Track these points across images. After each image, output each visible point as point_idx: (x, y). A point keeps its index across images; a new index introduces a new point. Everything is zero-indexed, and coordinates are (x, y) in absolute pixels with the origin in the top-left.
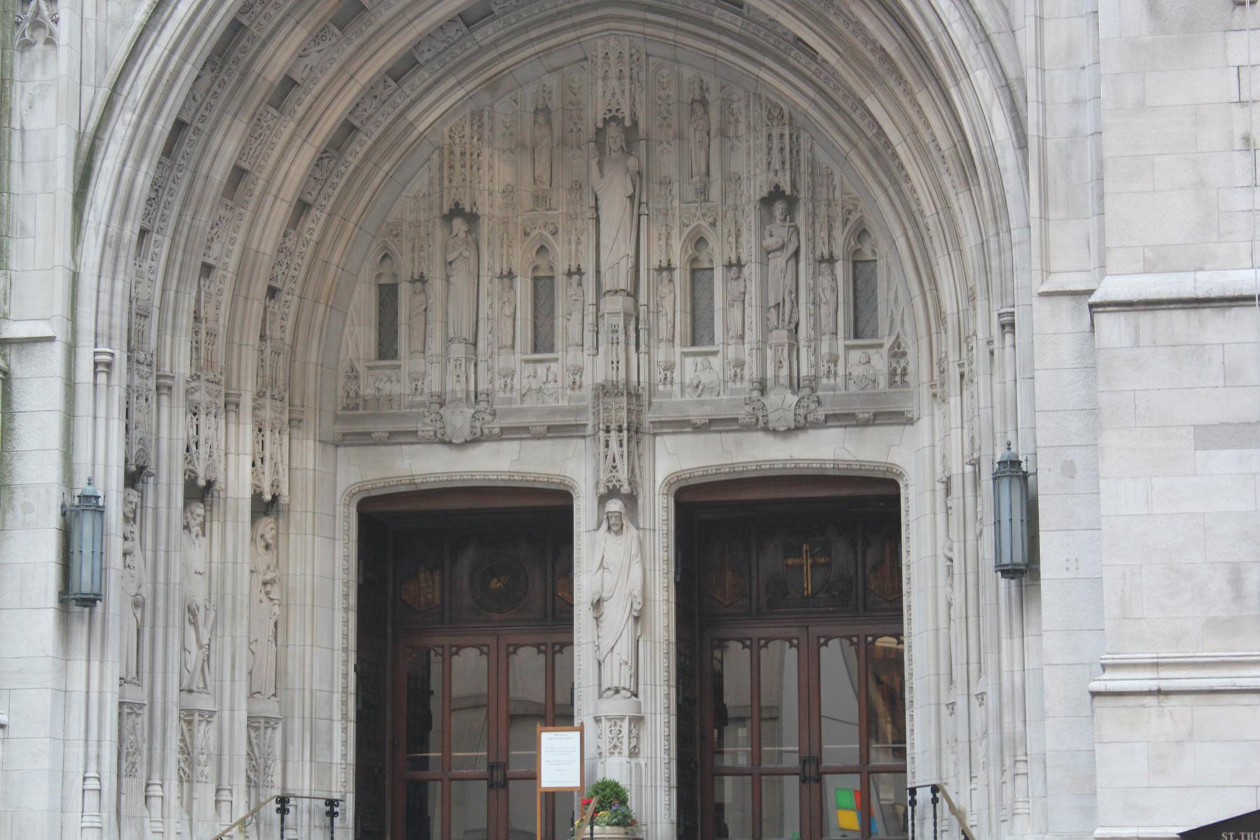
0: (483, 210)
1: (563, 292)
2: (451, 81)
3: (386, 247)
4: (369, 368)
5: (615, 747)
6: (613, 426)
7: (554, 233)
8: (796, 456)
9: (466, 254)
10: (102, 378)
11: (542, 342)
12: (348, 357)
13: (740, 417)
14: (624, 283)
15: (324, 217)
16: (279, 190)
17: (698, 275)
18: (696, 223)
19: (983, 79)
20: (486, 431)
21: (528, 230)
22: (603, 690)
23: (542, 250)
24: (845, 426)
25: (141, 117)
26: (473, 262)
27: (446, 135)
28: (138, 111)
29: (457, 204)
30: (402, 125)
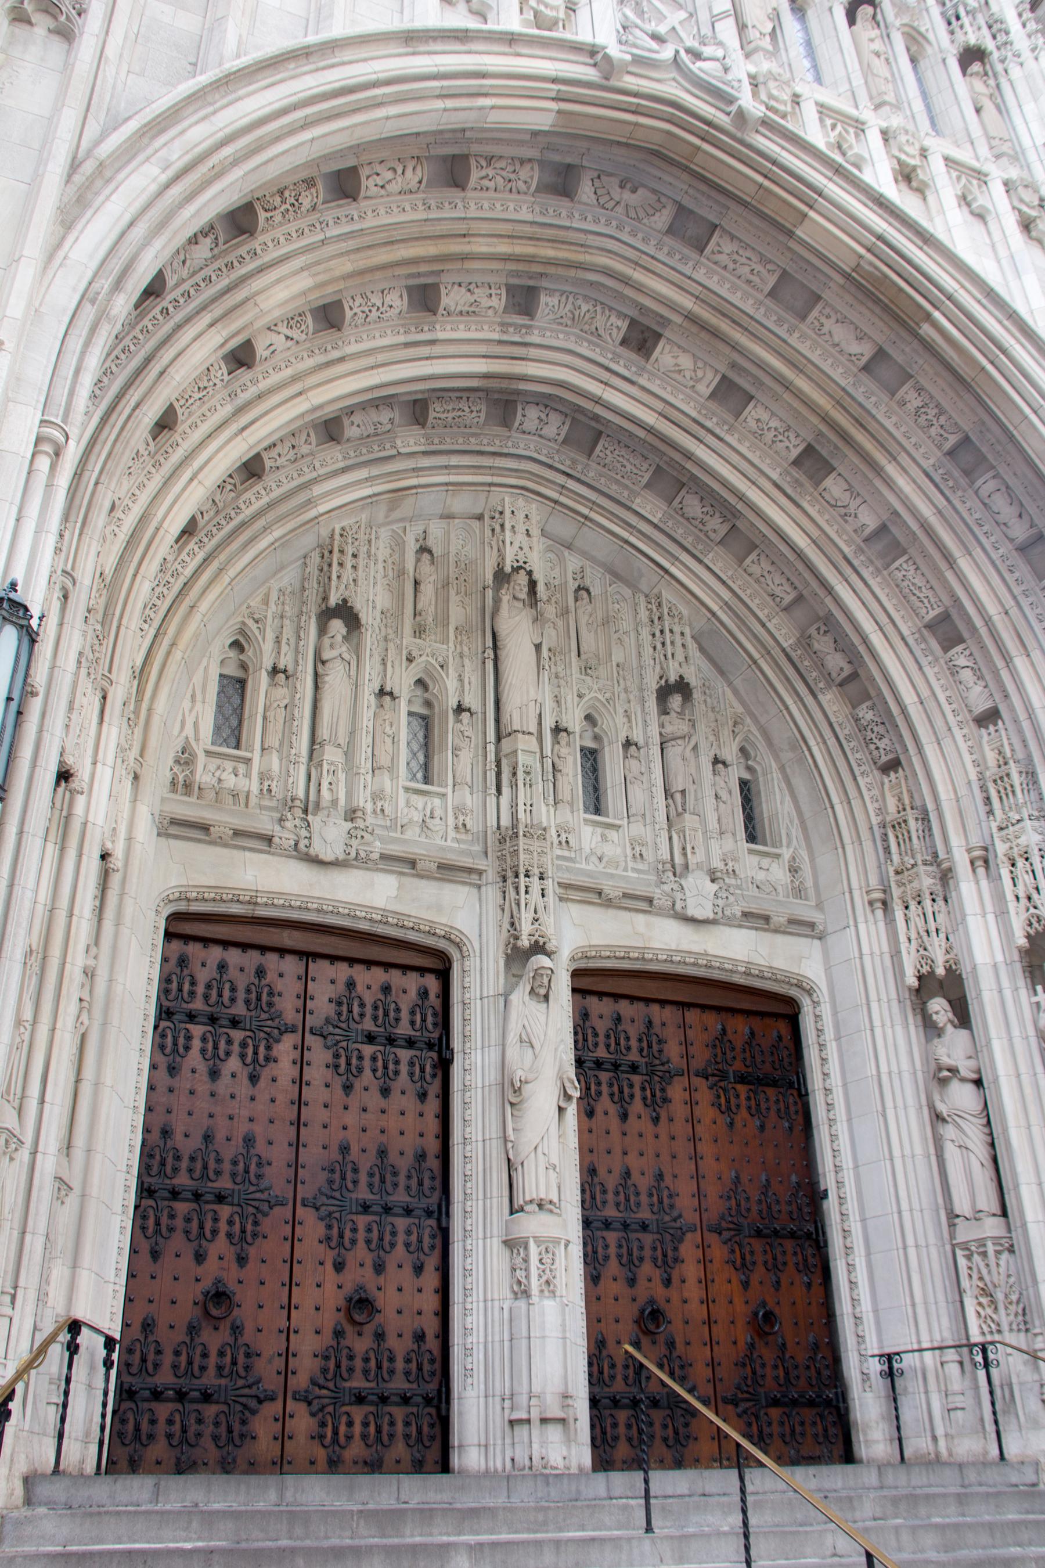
0: (368, 617)
1: (451, 730)
2: (362, 473)
3: (242, 632)
4: (208, 753)
5: (548, 1282)
6: (536, 871)
8: (711, 952)
9: (346, 656)
10: (44, 463)
12: (184, 734)
13: (656, 896)
15: (201, 556)
16: (201, 468)
18: (593, 694)
20: (363, 854)
21: (414, 654)
22: (519, 1201)
24: (757, 929)
25: (167, 186)
26: (354, 664)
27: (337, 532)
28: (170, 173)
29: (345, 601)
30: (302, 497)
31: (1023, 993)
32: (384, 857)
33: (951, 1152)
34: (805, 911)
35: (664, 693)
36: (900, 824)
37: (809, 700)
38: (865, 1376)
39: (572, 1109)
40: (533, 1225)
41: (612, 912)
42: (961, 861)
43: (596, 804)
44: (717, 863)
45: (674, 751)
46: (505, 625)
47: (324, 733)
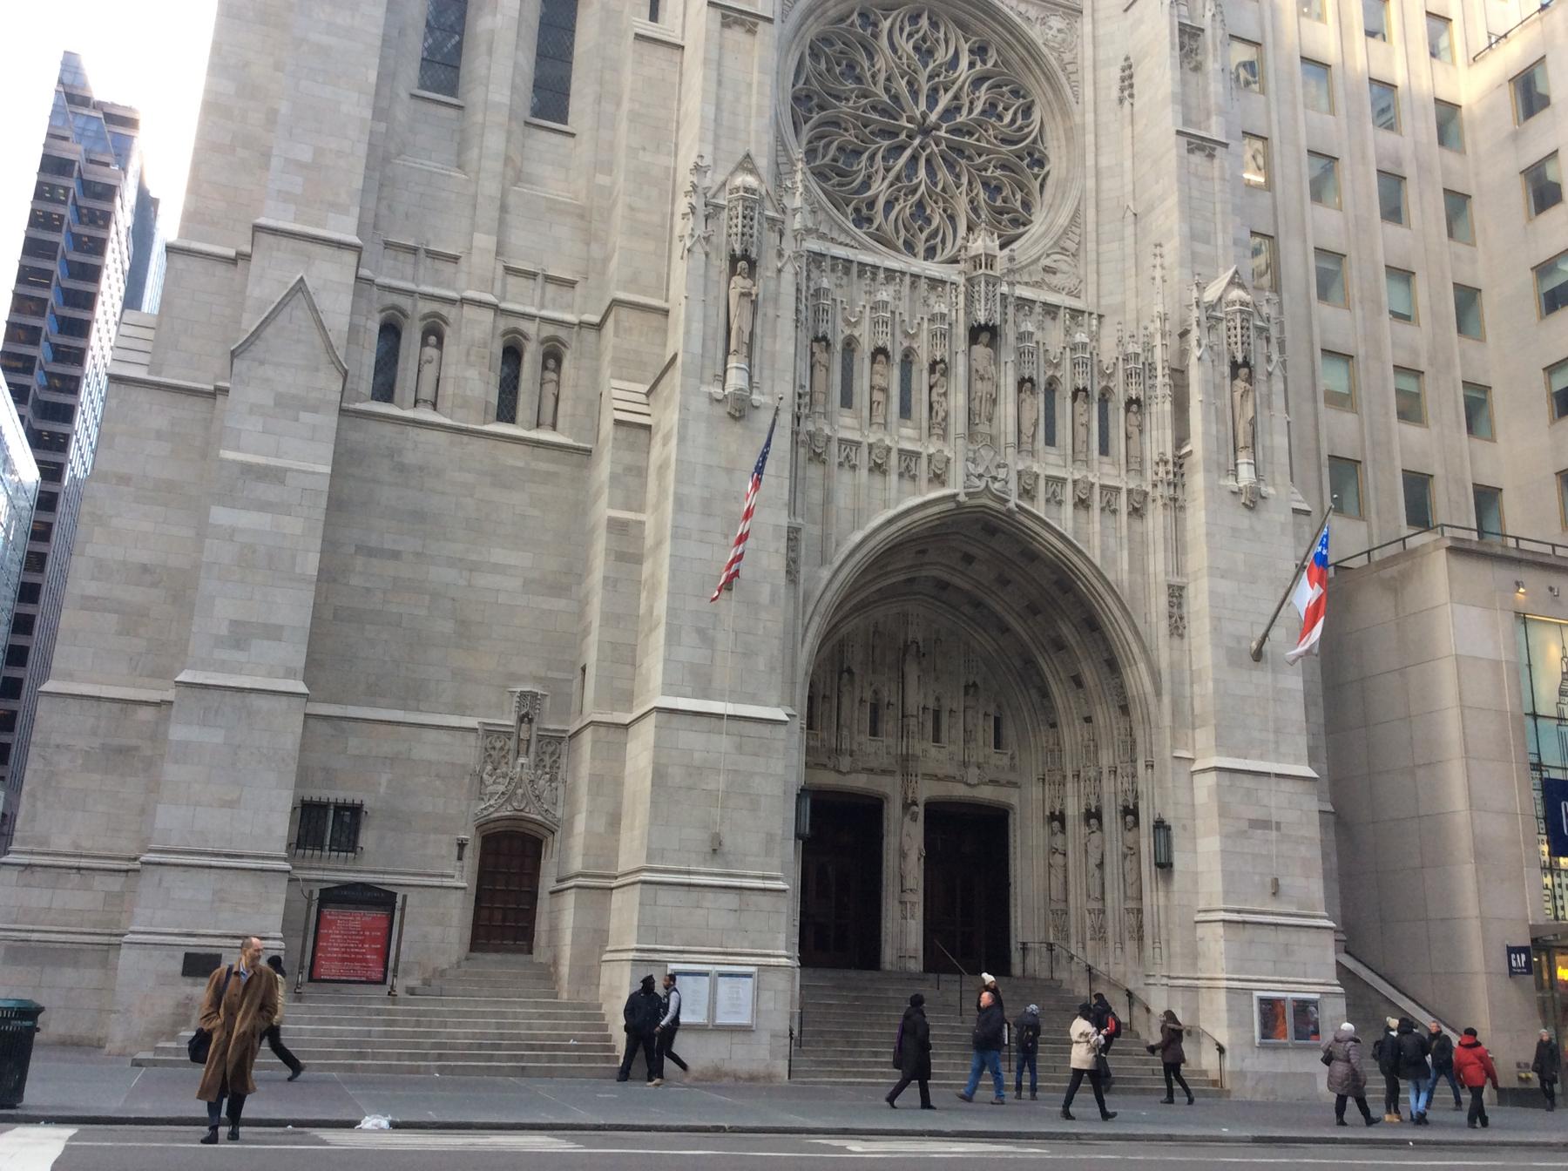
7: (883, 686)
11: (874, 732)
14: (915, 713)
17: (937, 716)
19: (1142, 666)
23: (875, 692)
31: (1083, 827)
32: (863, 769)
33: (1052, 877)
34: (1012, 777)
35: (967, 687)
36: (1052, 751)
37: (1025, 693)
38: (1017, 949)
39: (922, 860)
40: (909, 897)
41: (941, 782)
42: (1069, 774)
43: (936, 739)
44: (981, 760)
45: (970, 713)
46: (907, 669)
47: (842, 722)
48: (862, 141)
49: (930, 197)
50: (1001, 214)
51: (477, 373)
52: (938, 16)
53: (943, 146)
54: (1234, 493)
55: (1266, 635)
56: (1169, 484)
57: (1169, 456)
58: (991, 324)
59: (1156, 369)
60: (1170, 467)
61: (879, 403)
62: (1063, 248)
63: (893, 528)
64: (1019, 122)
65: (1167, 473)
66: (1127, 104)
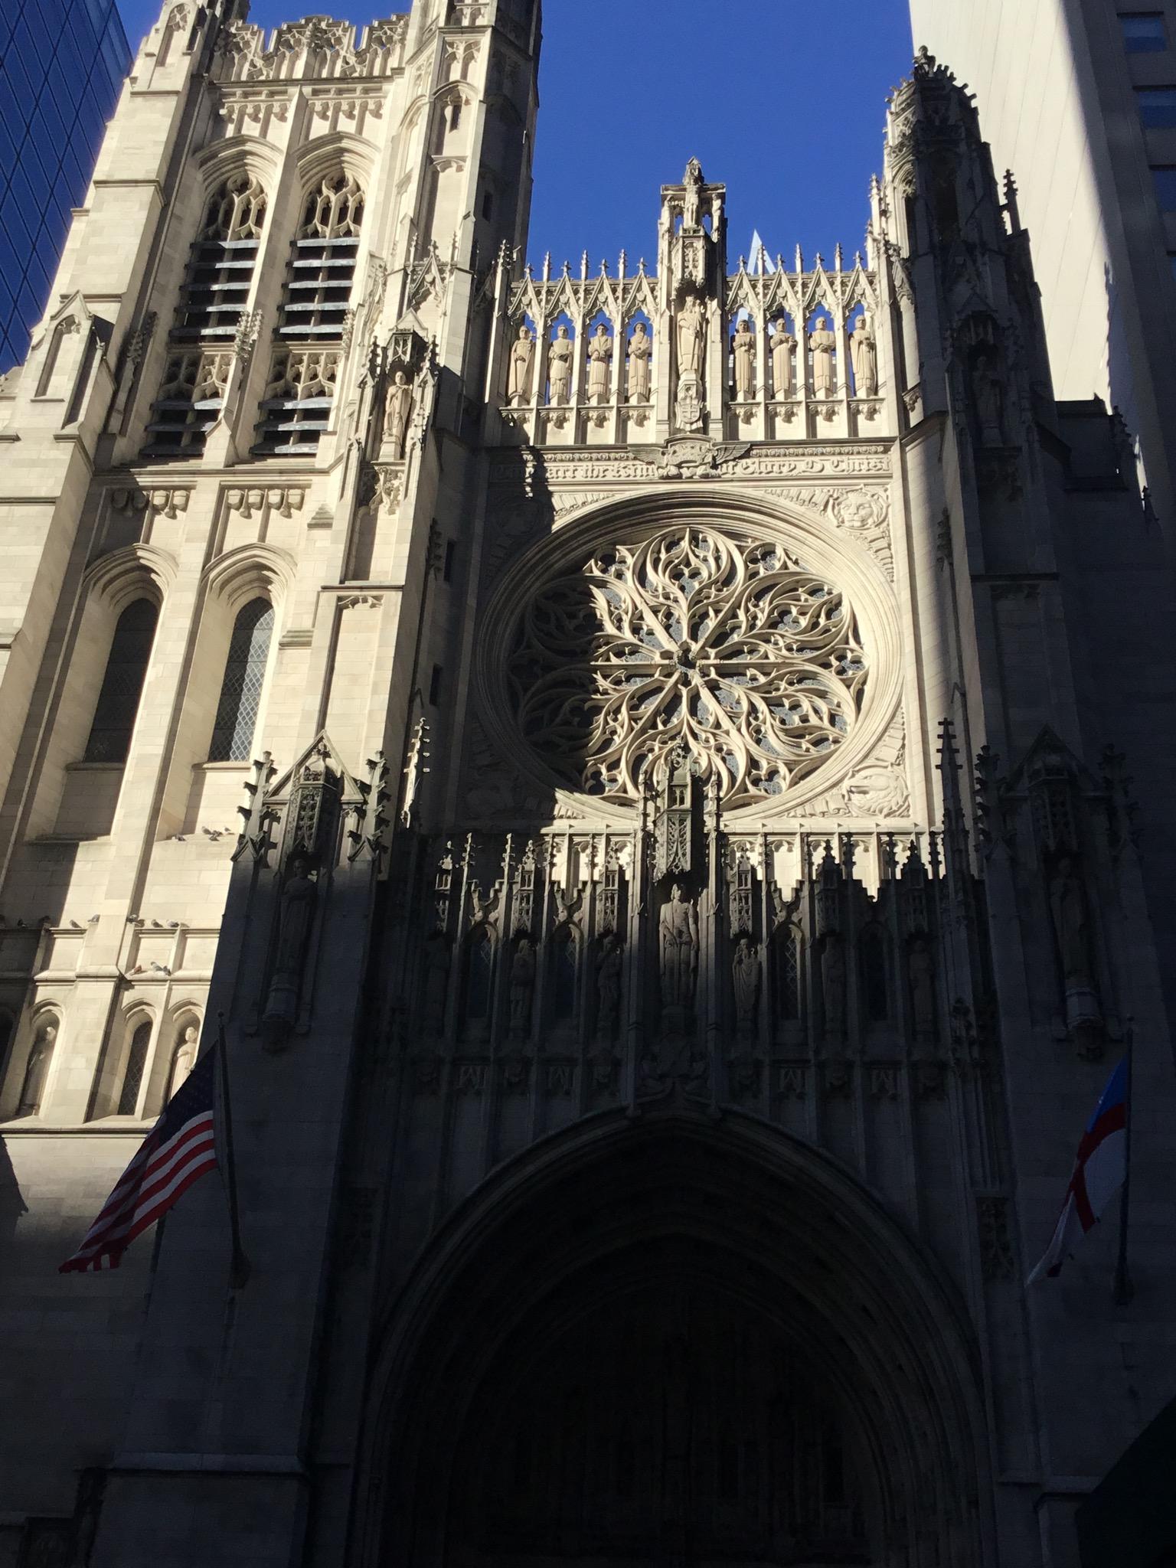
48: (602, 694)
49: (695, 736)
50: (802, 736)
51: (84, 1060)
52: (702, 532)
53: (713, 675)
54: (1060, 1040)
55: (1123, 1257)
56: (971, 1044)
57: (969, 1001)
58: (676, 871)
59: (948, 886)
60: (972, 1018)
61: (518, 1002)
62: (877, 759)
63: (530, 1169)
64: (822, 621)
65: (969, 1027)
66: (946, 563)
